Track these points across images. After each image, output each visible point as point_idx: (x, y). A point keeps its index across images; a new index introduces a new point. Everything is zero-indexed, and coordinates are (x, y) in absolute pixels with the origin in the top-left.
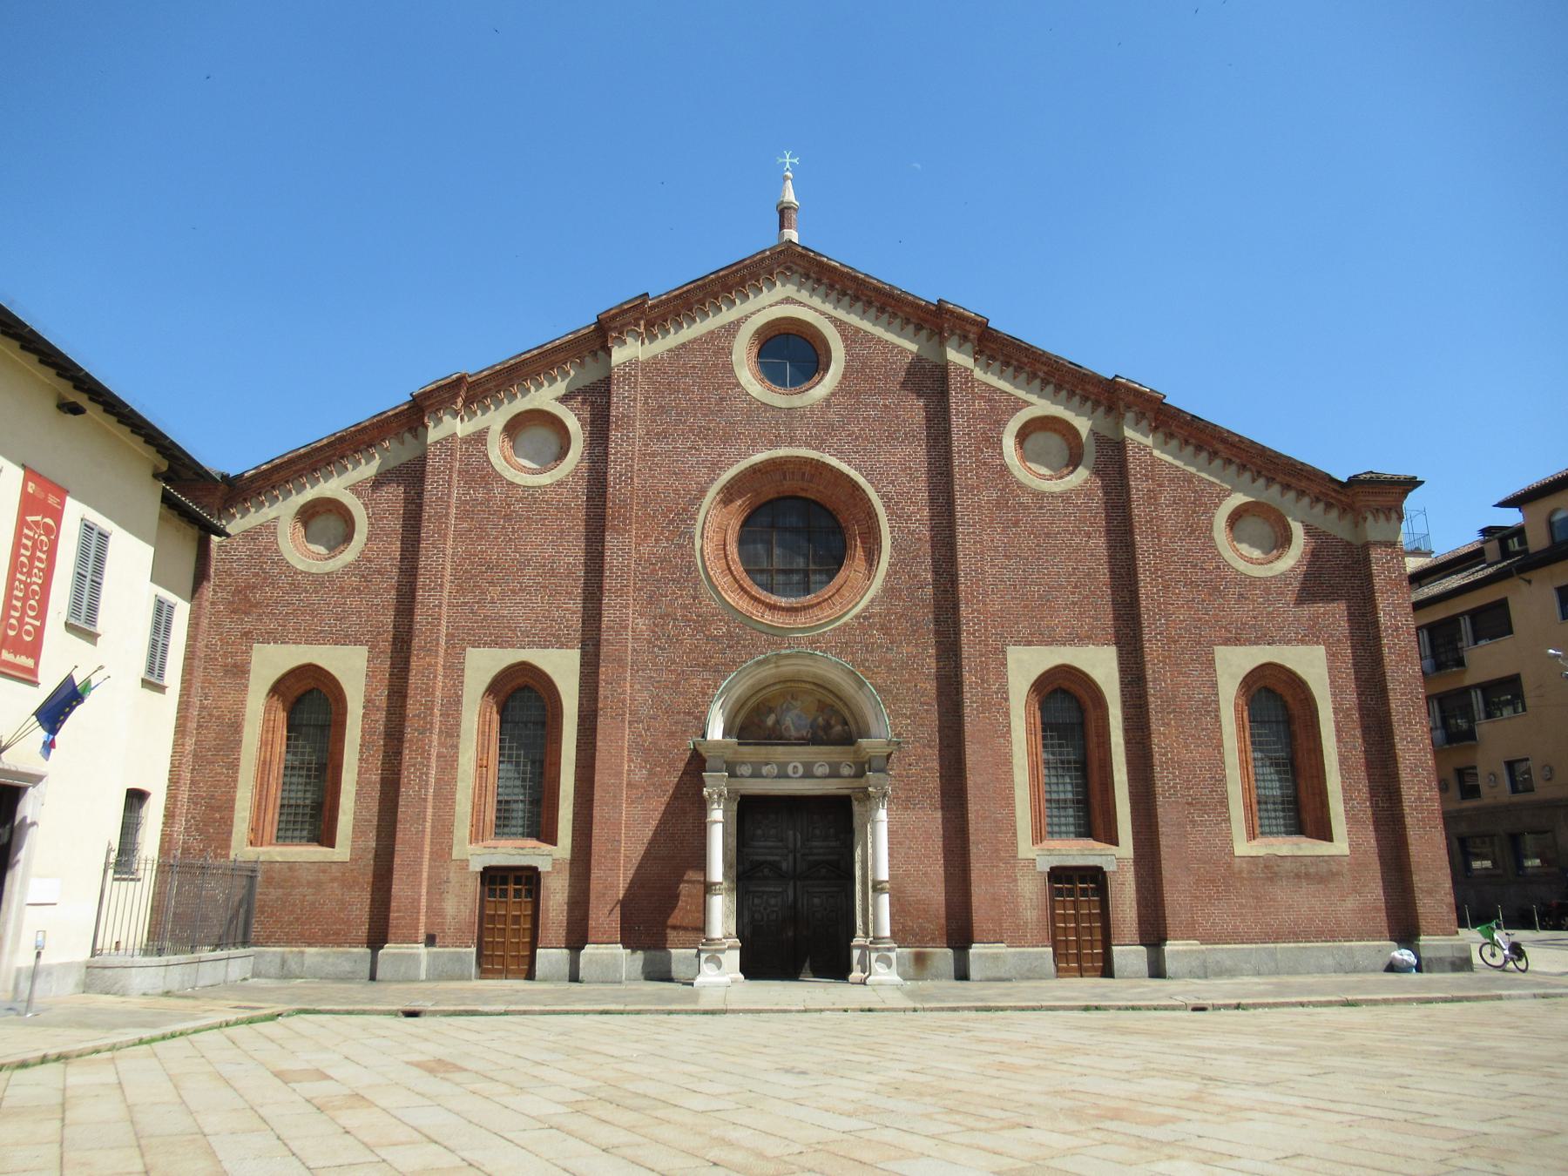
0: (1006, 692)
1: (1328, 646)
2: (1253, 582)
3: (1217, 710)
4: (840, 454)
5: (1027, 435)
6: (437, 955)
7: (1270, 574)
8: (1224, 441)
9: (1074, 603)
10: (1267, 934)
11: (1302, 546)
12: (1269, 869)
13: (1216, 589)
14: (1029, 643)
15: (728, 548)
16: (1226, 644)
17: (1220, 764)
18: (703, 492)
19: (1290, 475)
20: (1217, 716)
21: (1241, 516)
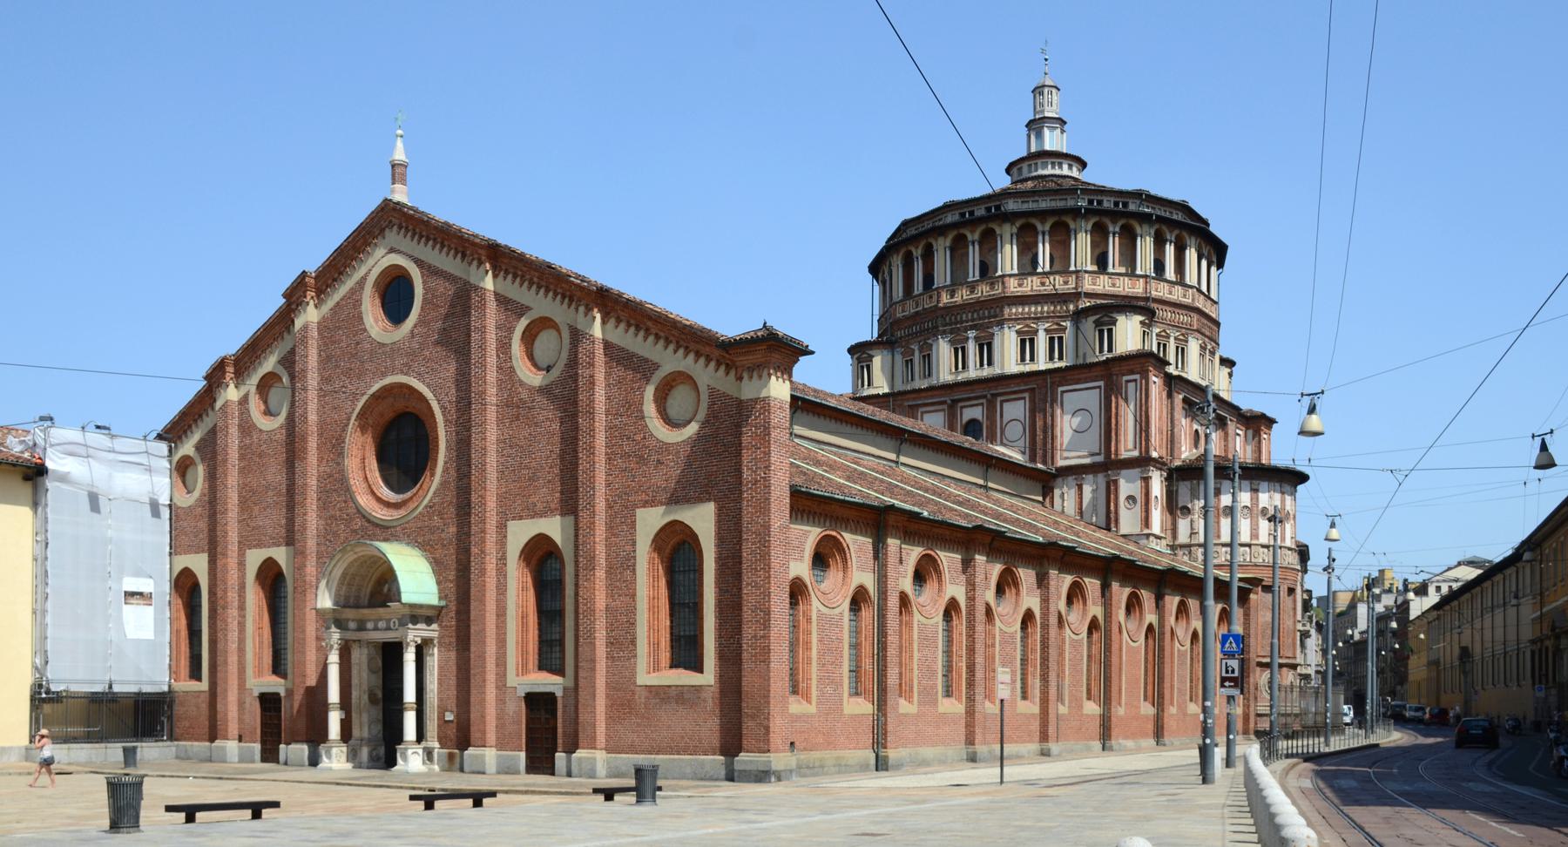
0: (505, 559)
1: (715, 501)
2: (665, 447)
3: (634, 565)
4: (420, 377)
5: (536, 336)
6: (243, 747)
7: (680, 439)
8: (650, 318)
9: (549, 481)
10: (652, 747)
11: (706, 410)
12: (660, 694)
13: (641, 457)
14: (521, 518)
15: (366, 461)
16: (644, 507)
17: (632, 611)
18: (349, 419)
19: (697, 342)
20: (634, 569)
21: (672, 387)
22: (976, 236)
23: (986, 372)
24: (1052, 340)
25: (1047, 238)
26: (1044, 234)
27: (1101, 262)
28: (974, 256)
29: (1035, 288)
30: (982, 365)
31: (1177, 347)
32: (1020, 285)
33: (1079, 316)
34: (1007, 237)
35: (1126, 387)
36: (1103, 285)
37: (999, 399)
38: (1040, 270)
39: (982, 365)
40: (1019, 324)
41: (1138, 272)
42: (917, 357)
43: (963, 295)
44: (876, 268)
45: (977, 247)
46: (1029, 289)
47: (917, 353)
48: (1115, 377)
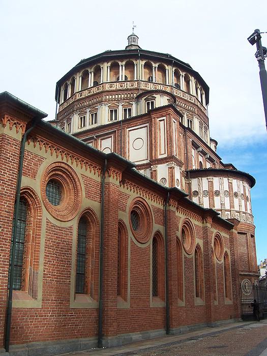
22: (92, 70)
23: (95, 126)
24: (125, 110)
25: (124, 68)
26: (122, 66)
27: (150, 80)
28: (91, 78)
29: (117, 88)
30: (92, 124)
31: (188, 120)
32: (111, 87)
33: (139, 98)
34: (105, 68)
35: (159, 123)
36: (150, 87)
37: (100, 138)
38: (120, 80)
39: (92, 124)
40: (109, 103)
41: (167, 84)
42: (65, 128)
43: (86, 94)
44: (57, 98)
45: (93, 74)
46: (115, 88)
47: (66, 123)
48: (153, 119)
